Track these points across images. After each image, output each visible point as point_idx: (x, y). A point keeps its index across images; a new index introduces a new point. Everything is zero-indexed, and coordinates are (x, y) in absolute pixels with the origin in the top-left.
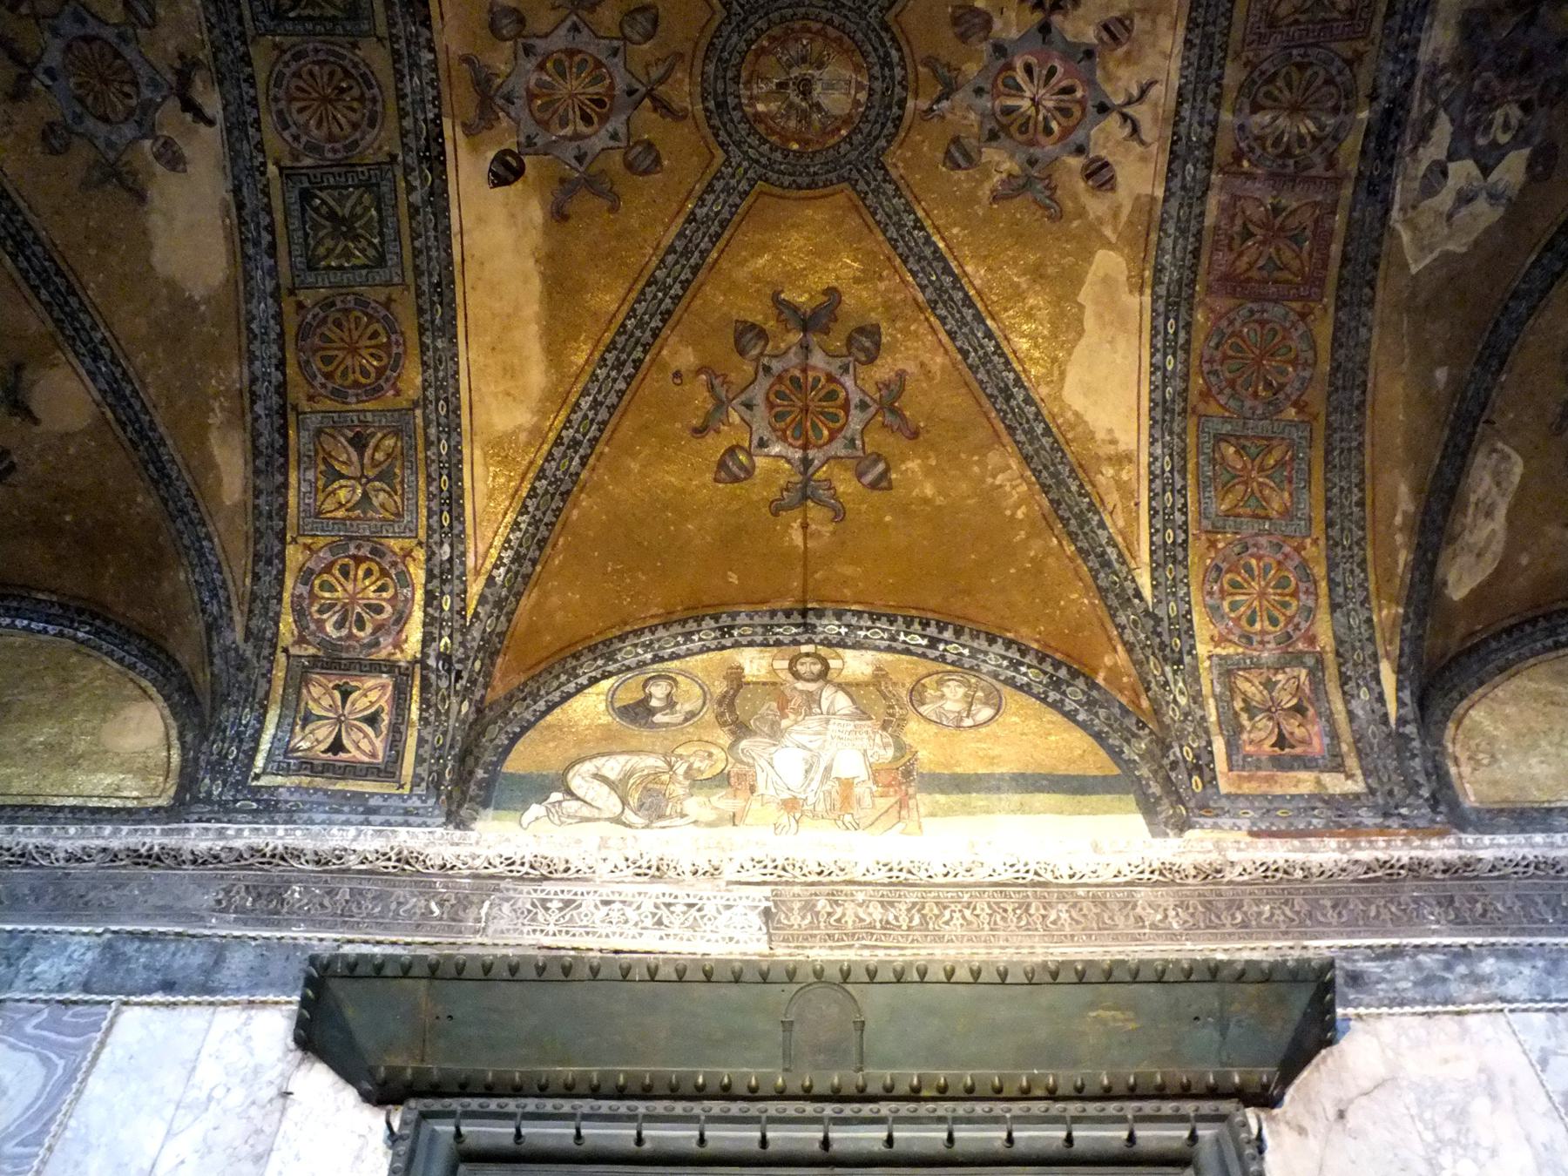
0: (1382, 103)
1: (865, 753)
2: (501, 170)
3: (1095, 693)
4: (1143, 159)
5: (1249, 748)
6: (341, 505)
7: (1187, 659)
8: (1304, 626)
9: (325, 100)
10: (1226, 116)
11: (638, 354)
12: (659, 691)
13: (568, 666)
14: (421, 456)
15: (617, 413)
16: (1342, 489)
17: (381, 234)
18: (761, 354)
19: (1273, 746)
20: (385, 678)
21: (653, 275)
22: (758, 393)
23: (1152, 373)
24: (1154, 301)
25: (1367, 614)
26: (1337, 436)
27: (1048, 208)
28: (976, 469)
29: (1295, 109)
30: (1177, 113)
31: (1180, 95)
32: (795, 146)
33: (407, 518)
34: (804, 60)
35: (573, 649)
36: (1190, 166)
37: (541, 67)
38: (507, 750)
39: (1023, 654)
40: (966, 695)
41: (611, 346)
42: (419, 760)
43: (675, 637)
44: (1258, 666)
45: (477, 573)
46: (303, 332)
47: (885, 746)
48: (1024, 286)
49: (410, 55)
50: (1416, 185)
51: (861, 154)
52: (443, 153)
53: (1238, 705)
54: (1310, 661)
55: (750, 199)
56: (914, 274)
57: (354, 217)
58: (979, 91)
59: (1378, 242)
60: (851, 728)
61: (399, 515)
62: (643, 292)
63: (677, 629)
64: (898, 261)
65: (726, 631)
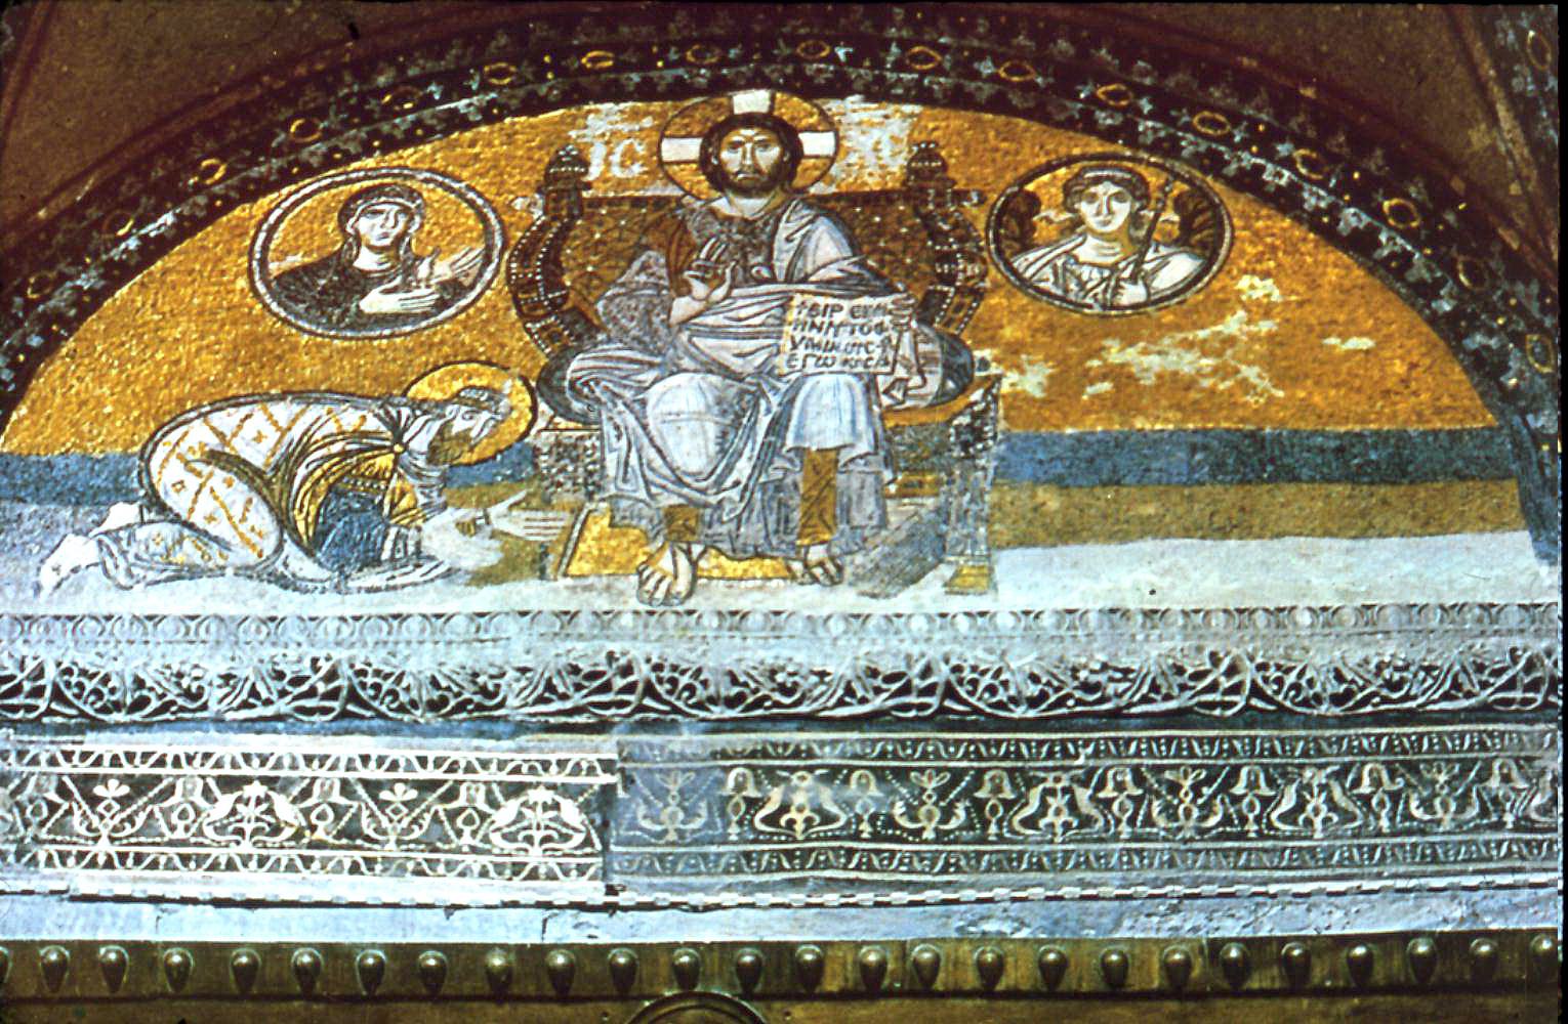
1: (870, 387)
40: (1134, 219)
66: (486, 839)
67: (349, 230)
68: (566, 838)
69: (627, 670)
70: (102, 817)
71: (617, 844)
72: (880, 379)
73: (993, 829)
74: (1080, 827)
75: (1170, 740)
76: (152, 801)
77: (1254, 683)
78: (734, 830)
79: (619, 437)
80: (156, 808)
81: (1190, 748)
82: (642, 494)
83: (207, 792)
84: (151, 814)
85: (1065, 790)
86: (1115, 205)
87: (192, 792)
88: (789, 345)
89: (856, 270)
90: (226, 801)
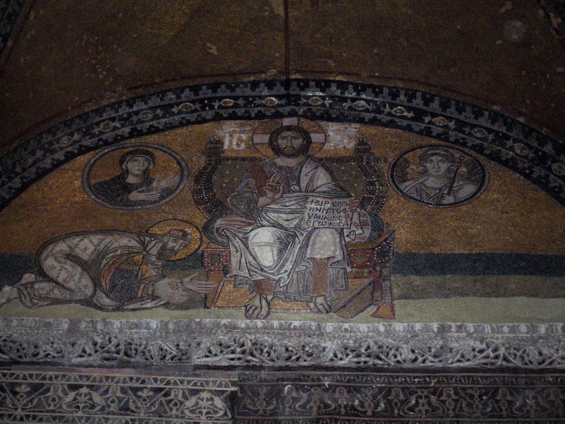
1: (341, 233)
13: (44, 141)
39: (509, 129)
40: (448, 170)
47: (362, 225)
60: (328, 206)
63: (155, 101)
66: (182, 412)
67: (124, 167)
68: (216, 412)
69: (243, 345)
70: (19, 400)
71: (238, 415)
72: (345, 230)
73: (396, 411)
74: (433, 411)
75: (469, 377)
76: (40, 394)
77: (504, 354)
78: (287, 410)
79: (237, 251)
80: (42, 397)
81: (478, 381)
82: (248, 275)
83: (64, 391)
84: (40, 399)
85: (426, 397)
86: (440, 164)
87: (57, 391)
88: (307, 217)
89: (334, 188)
90: (72, 395)
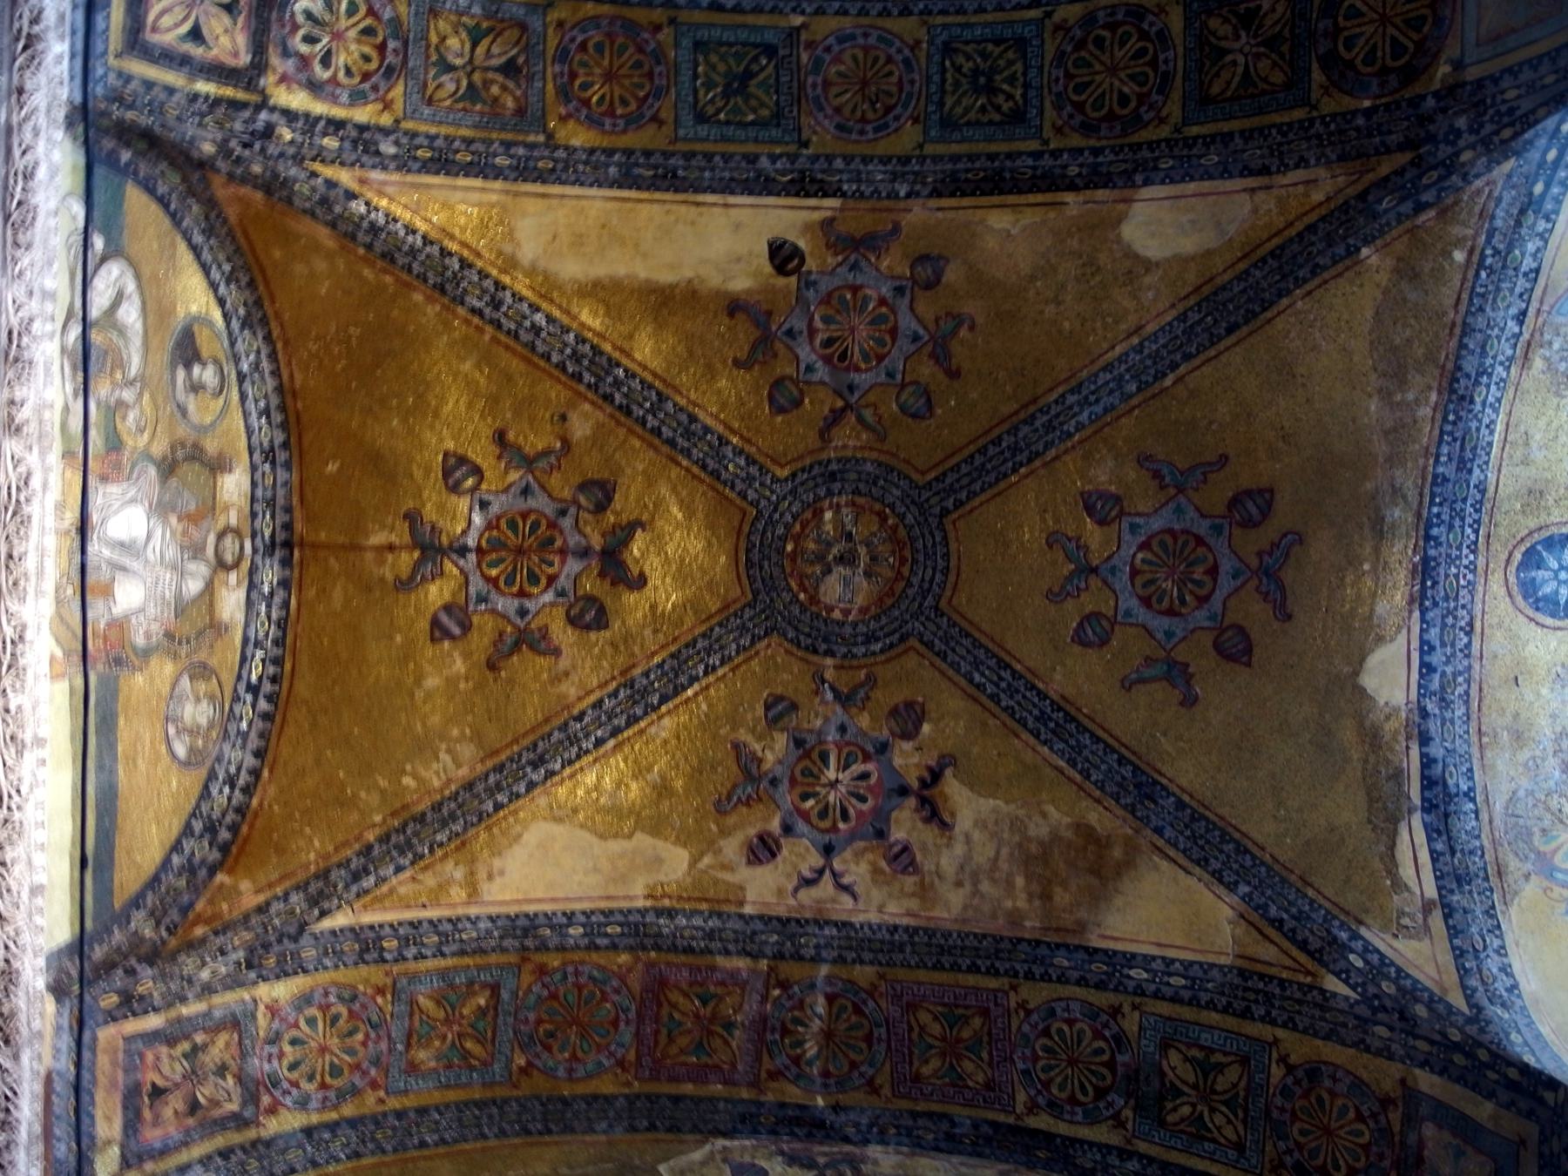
0: (830, 1118)
2: (787, 249)
3: (203, 873)
4: (780, 892)
5: (150, 1057)
6: (443, 39)
7: (252, 975)
8: (288, 1101)
9: (865, 84)
10: (824, 970)
11: (587, 377)
12: (208, 375)
14: (494, 135)
15: (525, 352)
16: (437, 1123)
17: (728, 123)
18: (580, 507)
19: (154, 1085)
20: (245, 59)
21: (668, 398)
22: (539, 502)
23: (564, 914)
24: (639, 911)
25: (298, 1167)
26: (495, 1110)
27: (729, 798)
28: (455, 732)
29: (828, 1035)
30: (827, 922)
31: (845, 924)
32: (789, 548)
33: (427, 111)
34: (874, 559)
35: (259, 279)
36: (775, 938)
37: (882, 302)
38: (150, 190)
40: (199, 727)
41: (596, 350)
42: (149, 85)
43: (266, 396)
44: (243, 1055)
45: (362, 182)
46: (631, 27)
48: (649, 777)
49: (904, 174)
50: (747, 1159)
51: (780, 613)
52: (807, 195)
53: (199, 1038)
54: (248, 1114)
55: (738, 501)
56: (660, 665)
57: (748, 97)
58: (842, 729)
59: (695, 1129)
61: (430, 102)
62: (651, 387)
64: (673, 649)
65: (269, 455)
